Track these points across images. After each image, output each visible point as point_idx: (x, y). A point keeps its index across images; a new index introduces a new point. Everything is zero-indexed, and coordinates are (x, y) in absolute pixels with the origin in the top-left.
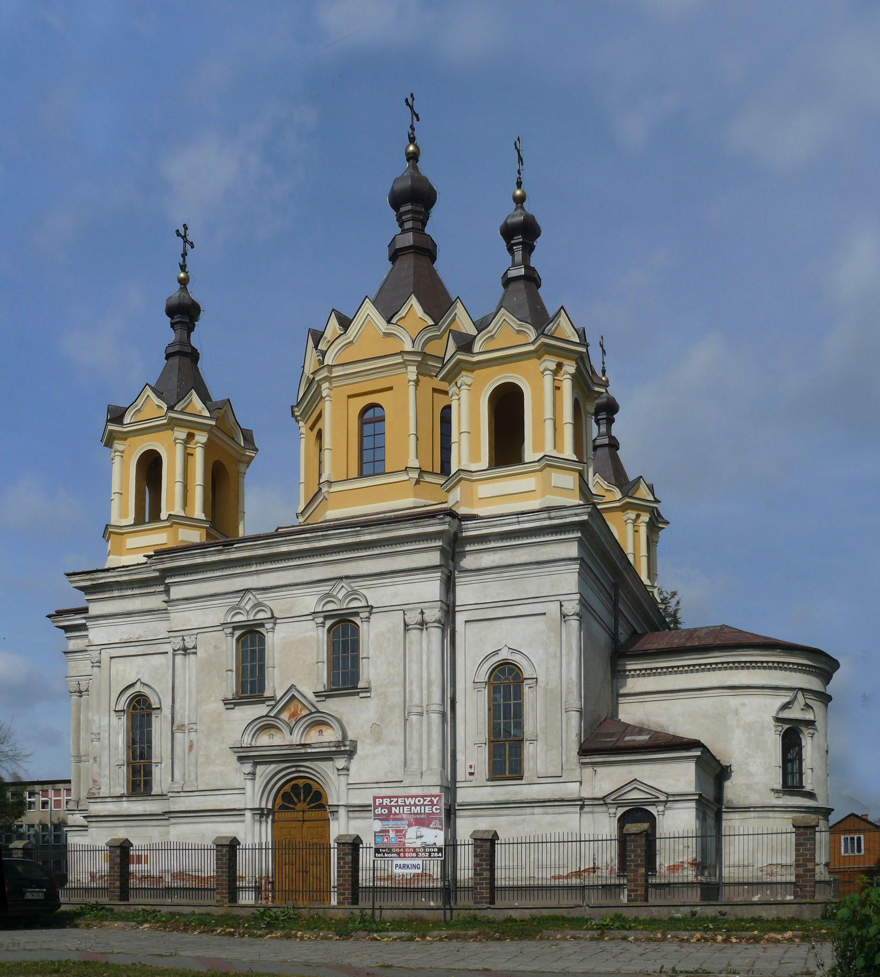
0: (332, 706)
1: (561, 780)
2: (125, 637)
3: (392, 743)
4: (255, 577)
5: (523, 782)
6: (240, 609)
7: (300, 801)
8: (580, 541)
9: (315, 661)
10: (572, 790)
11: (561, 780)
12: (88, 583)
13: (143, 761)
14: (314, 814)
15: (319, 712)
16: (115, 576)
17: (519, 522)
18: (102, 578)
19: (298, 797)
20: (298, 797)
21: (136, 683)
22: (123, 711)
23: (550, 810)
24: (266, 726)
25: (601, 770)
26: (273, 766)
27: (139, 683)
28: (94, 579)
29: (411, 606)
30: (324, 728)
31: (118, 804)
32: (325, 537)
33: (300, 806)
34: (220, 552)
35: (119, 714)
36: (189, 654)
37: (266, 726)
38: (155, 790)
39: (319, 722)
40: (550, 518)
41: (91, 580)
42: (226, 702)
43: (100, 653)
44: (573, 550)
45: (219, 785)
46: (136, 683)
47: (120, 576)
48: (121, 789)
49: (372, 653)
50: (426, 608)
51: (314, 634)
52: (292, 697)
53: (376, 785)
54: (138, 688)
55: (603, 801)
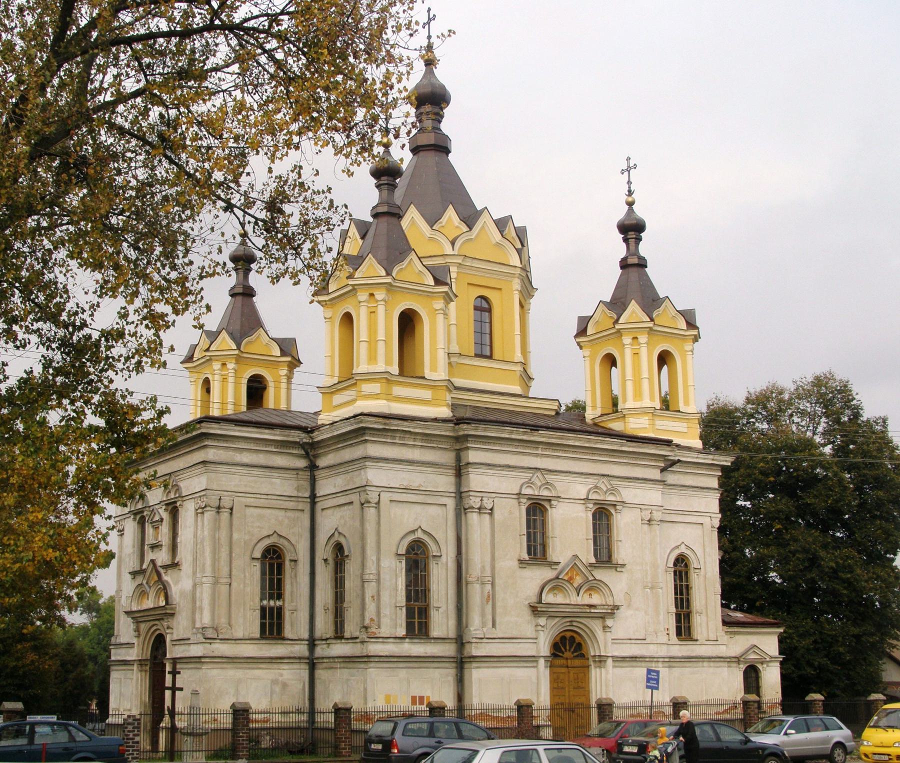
0: (599, 574)
1: (718, 643)
2: (405, 484)
3: (637, 609)
4: (539, 459)
5: (698, 643)
6: (531, 483)
7: (569, 650)
8: (719, 478)
9: (585, 537)
10: (722, 651)
11: (718, 643)
12: (381, 427)
13: (417, 603)
14: (577, 662)
15: (595, 579)
16: (409, 427)
17: (697, 458)
18: (396, 425)
19: (570, 647)
20: (570, 647)
21: (417, 530)
23: (712, 664)
24: (556, 585)
25: (737, 637)
26: (557, 619)
27: (419, 530)
28: (388, 425)
29: (646, 507)
30: (592, 593)
31: (401, 646)
32: (602, 442)
33: (568, 654)
34: (525, 433)
35: (401, 557)
36: (485, 513)
37: (556, 585)
38: (435, 632)
39: (594, 586)
40: (713, 460)
41: (385, 424)
42: (521, 561)
43: (379, 495)
44: (715, 483)
45: (515, 634)
46: (417, 530)
47: (415, 428)
48: (402, 632)
49: (621, 537)
50: (655, 510)
51: (583, 515)
52: (574, 564)
53: (629, 641)
54: (419, 535)
55: (737, 660)
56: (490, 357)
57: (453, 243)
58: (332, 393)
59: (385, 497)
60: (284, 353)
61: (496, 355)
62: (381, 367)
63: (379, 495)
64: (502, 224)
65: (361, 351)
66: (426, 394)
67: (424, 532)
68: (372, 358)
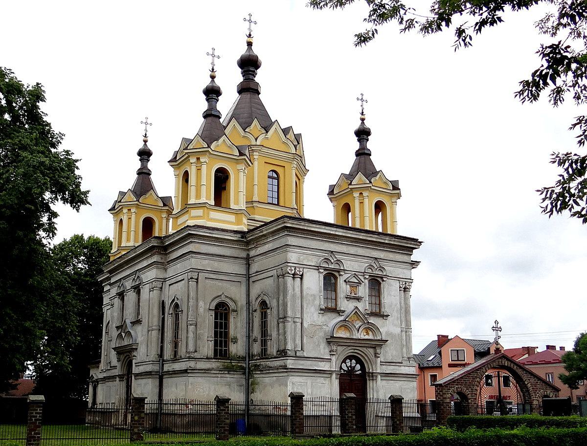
22: (213, 310)
43: (198, 274)
54: (223, 298)
56: (278, 205)
57: (256, 139)
58: (177, 218)
59: (202, 276)
60: (165, 205)
61: (281, 204)
62: (203, 200)
63: (198, 274)
64: (286, 131)
65: (192, 191)
66: (232, 218)
67: (226, 297)
68: (198, 196)
